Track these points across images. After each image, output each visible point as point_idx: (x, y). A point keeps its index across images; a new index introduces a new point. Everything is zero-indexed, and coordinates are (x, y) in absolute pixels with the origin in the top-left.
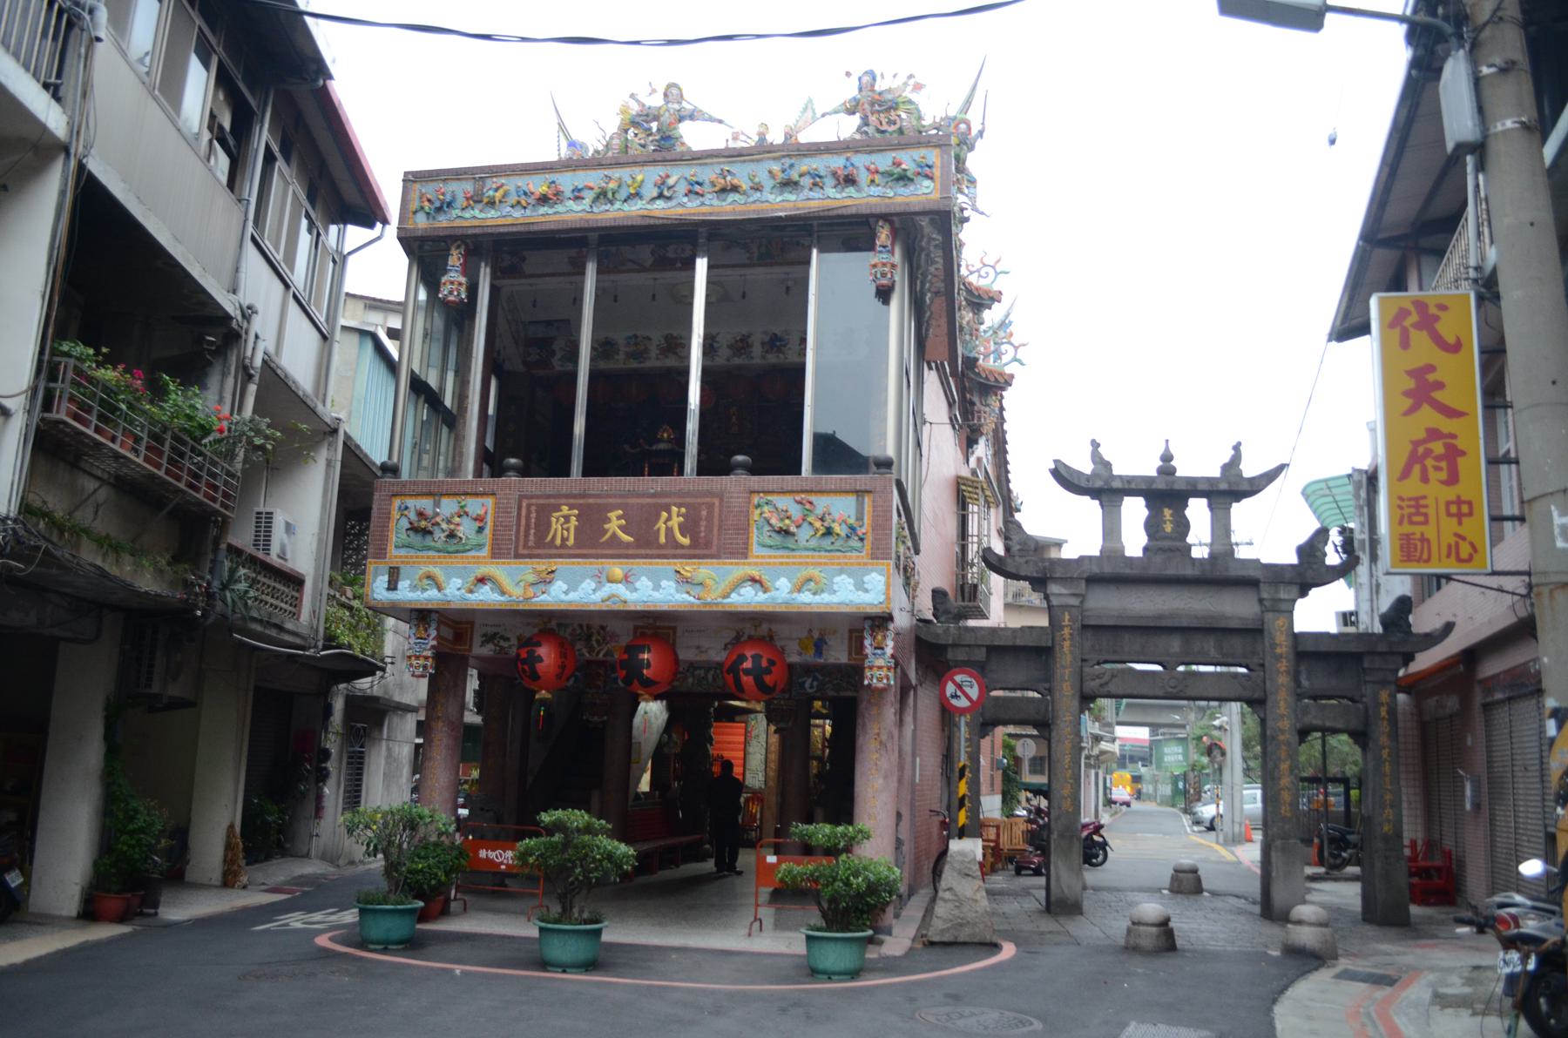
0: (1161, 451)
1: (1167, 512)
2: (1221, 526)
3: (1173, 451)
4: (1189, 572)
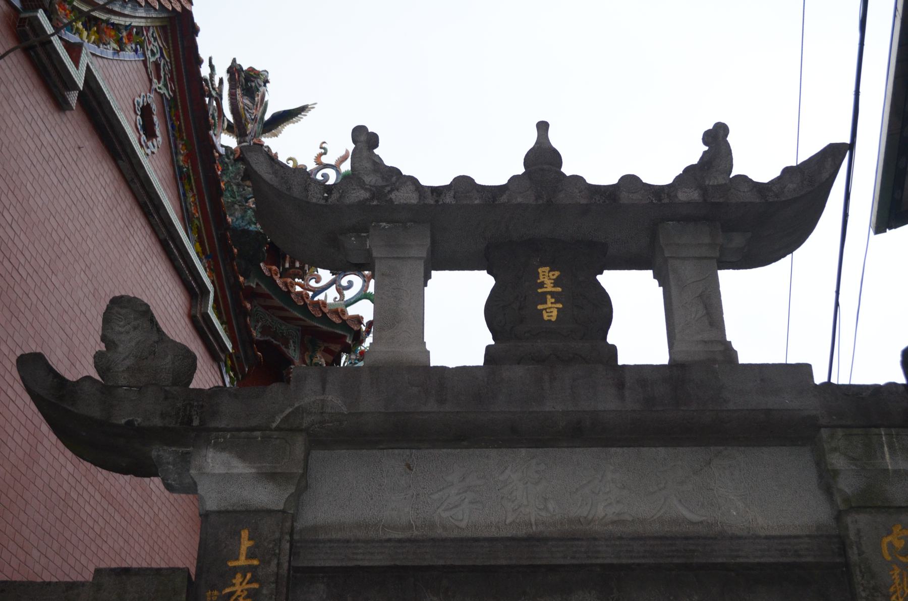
0: (530, 139)
1: (547, 277)
2: (695, 314)
3: (555, 139)
4: (607, 403)
